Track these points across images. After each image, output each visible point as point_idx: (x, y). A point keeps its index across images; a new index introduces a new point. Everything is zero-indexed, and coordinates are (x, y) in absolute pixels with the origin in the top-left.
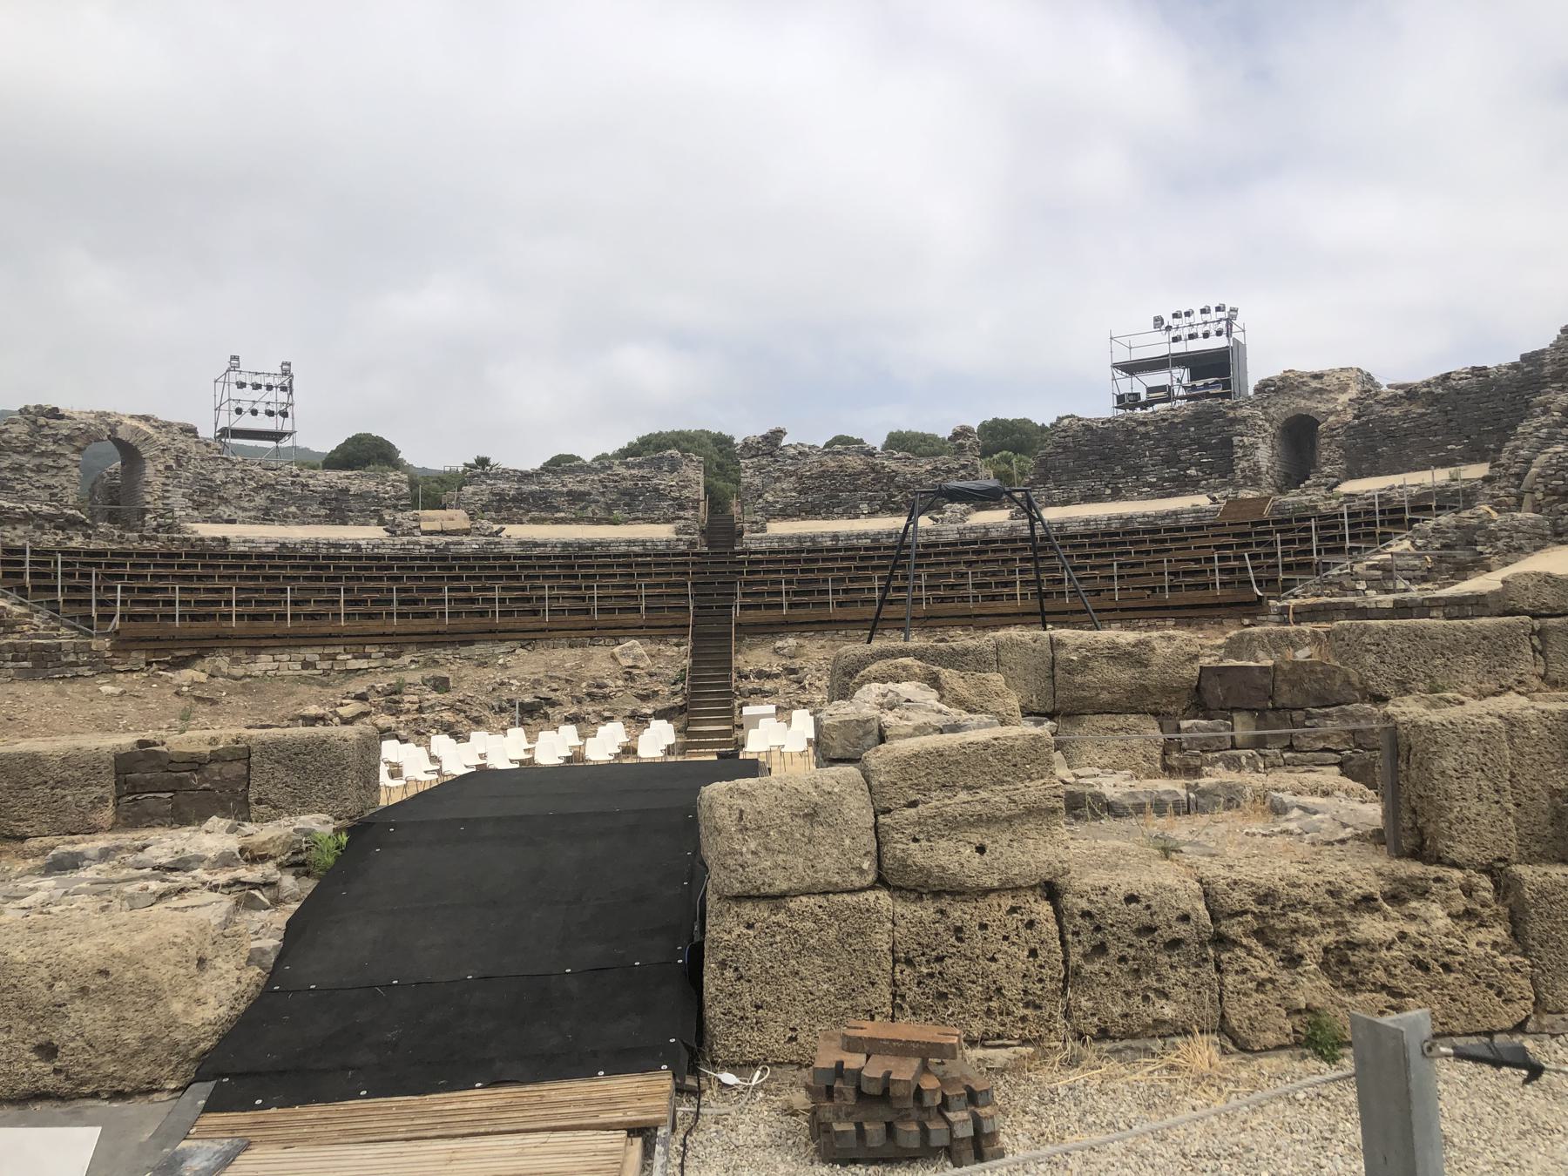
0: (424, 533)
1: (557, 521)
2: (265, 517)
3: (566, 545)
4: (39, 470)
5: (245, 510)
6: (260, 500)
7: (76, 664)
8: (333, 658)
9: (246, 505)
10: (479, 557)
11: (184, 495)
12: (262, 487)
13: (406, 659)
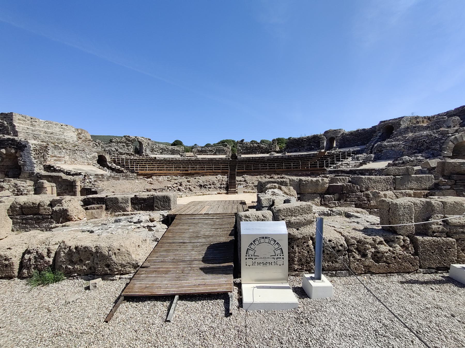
1: (207, 155)
2: (161, 153)
3: (209, 159)
6: (161, 151)
10: (195, 160)
13: (184, 177)
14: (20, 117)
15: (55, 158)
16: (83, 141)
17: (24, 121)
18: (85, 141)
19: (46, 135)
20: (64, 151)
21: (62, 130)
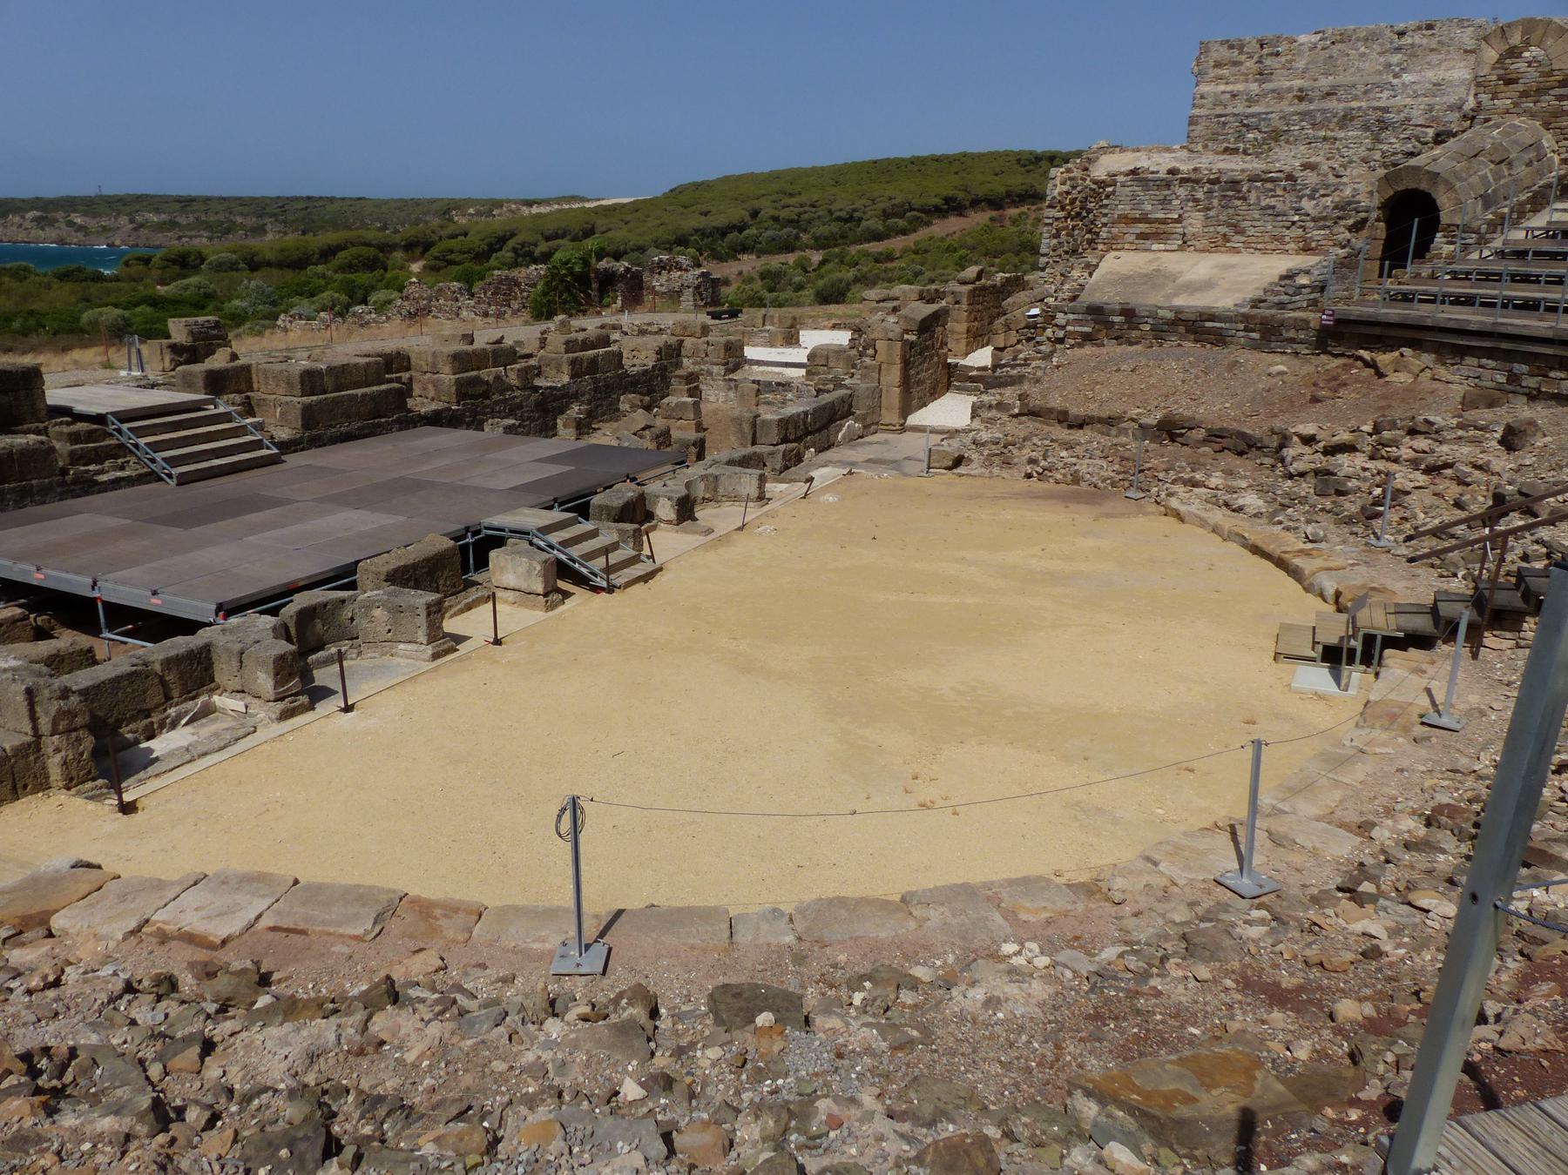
14: (1224, 53)
15: (1142, 227)
16: (1524, 94)
17: (1236, 64)
18: (1541, 91)
19: (1303, 107)
20: (1182, 192)
21: (1396, 58)
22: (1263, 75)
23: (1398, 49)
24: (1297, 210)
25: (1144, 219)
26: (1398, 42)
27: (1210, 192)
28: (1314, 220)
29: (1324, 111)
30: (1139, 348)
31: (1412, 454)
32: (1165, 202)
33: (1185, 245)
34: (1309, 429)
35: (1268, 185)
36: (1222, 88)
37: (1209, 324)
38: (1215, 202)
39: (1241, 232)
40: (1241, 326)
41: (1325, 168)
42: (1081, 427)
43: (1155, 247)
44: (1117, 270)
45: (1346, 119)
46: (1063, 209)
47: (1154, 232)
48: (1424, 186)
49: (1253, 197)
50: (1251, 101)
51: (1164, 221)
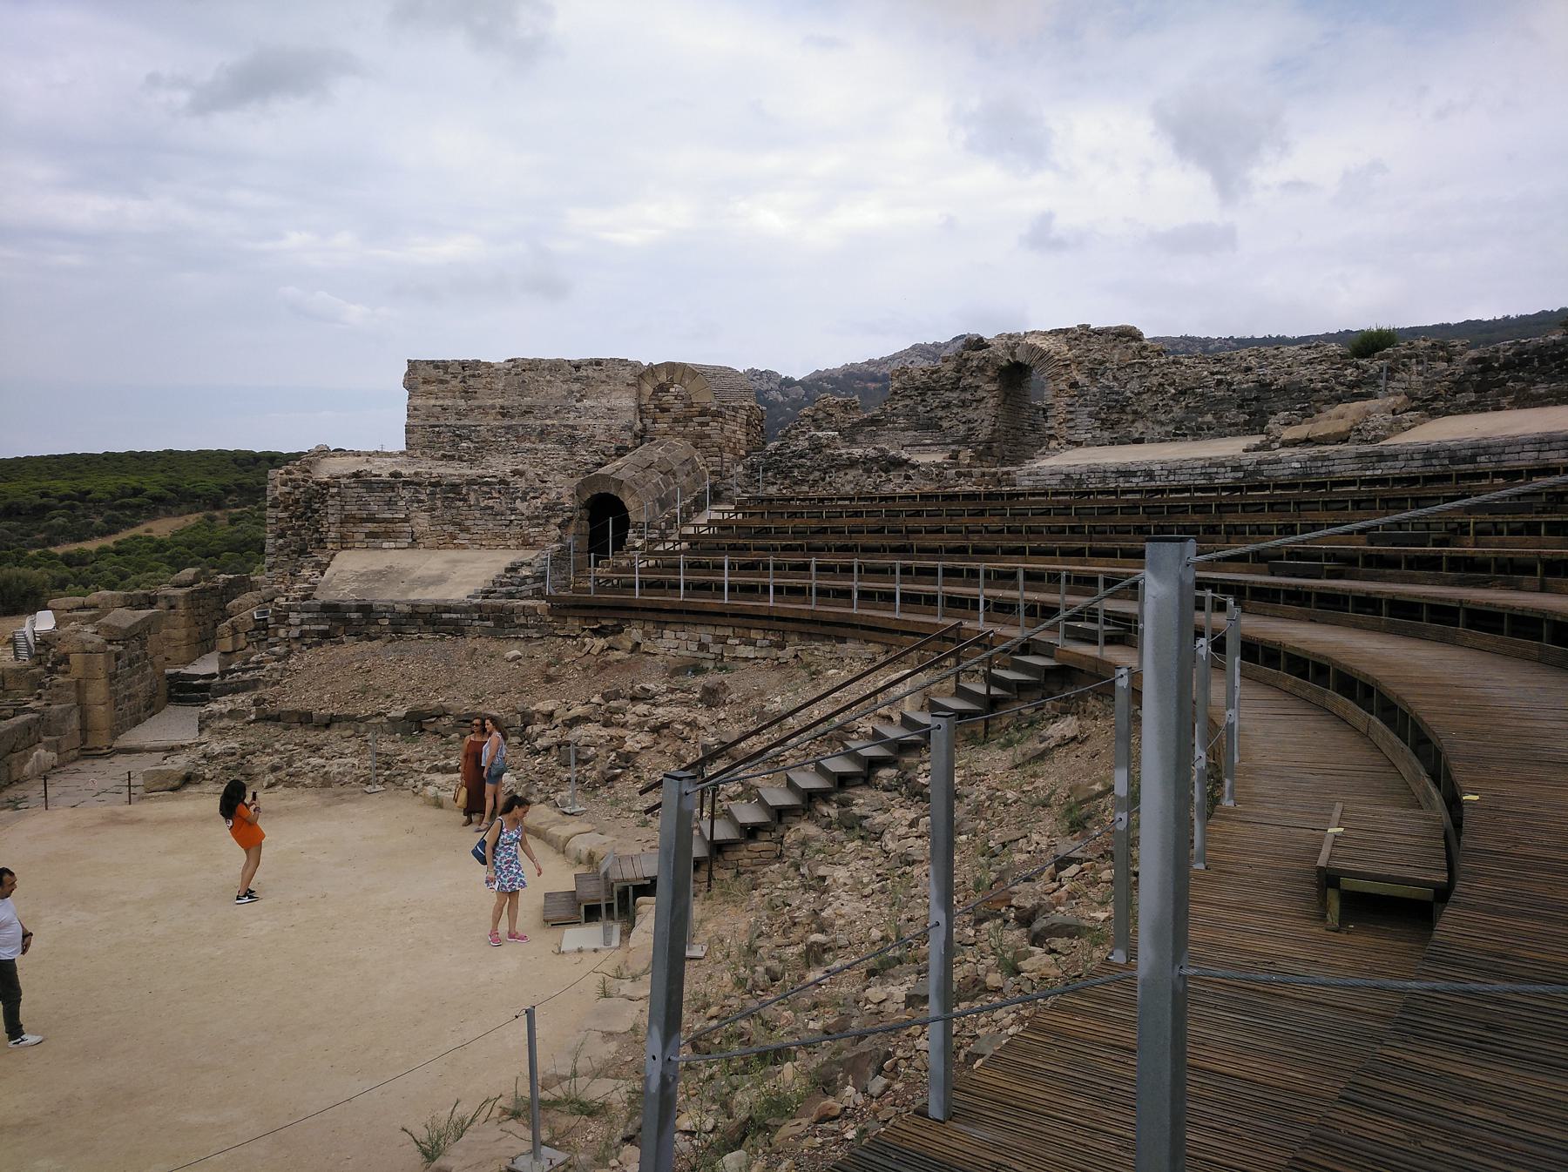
0: (1285, 444)
2: (1179, 432)
4: (964, 404)
5: (1162, 424)
6: (1178, 412)
7: (525, 626)
8: (722, 640)
9: (1163, 418)
11: (1090, 415)
12: (1183, 393)
15: (371, 527)
17: (442, 382)
19: (506, 422)
20: (406, 493)
21: (576, 387)
22: (467, 393)
23: (577, 380)
24: (513, 510)
25: (371, 519)
26: (576, 375)
27: (433, 494)
28: (528, 518)
29: (525, 427)
30: (376, 643)
31: (636, 719)
32: (390, 503)
33: (414, 543)
34: (546, 706)
35: (485, 489)
36: (433, 402)
37: (445, 616)
38: (439, 503)
39: (467, 530)
40: (476, 616)
41: (530, 474)
42: (327, 726)
43: (385, 545)
44: (349, 573)
45: (543, 434)
46: (286, 509)
47: (382, 533)
48: (613, 492)
49: (472, 499)
50: (460, 414)
51: (392, 521)
